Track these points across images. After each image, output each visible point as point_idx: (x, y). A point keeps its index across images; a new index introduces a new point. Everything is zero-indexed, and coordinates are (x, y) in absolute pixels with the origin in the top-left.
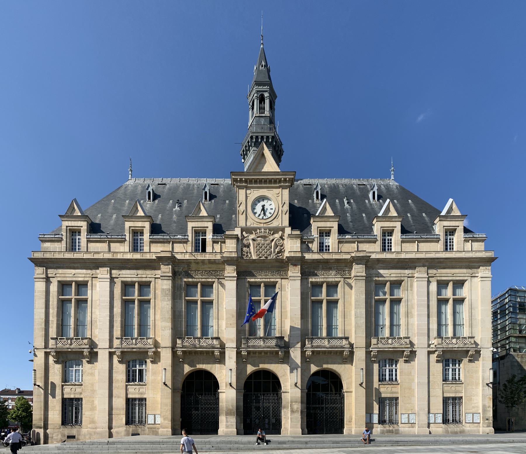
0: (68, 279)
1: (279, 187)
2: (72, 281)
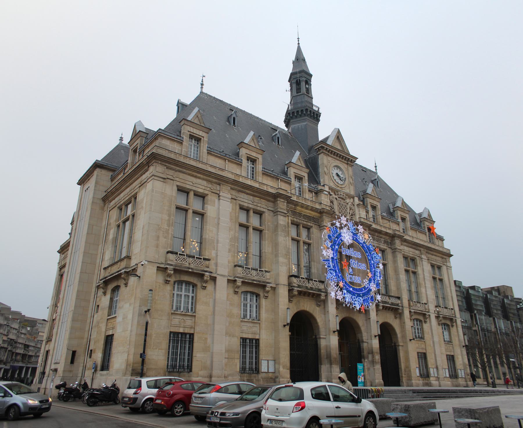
0: (188, 187)
1: (347, 164)
2: (191, 190)
